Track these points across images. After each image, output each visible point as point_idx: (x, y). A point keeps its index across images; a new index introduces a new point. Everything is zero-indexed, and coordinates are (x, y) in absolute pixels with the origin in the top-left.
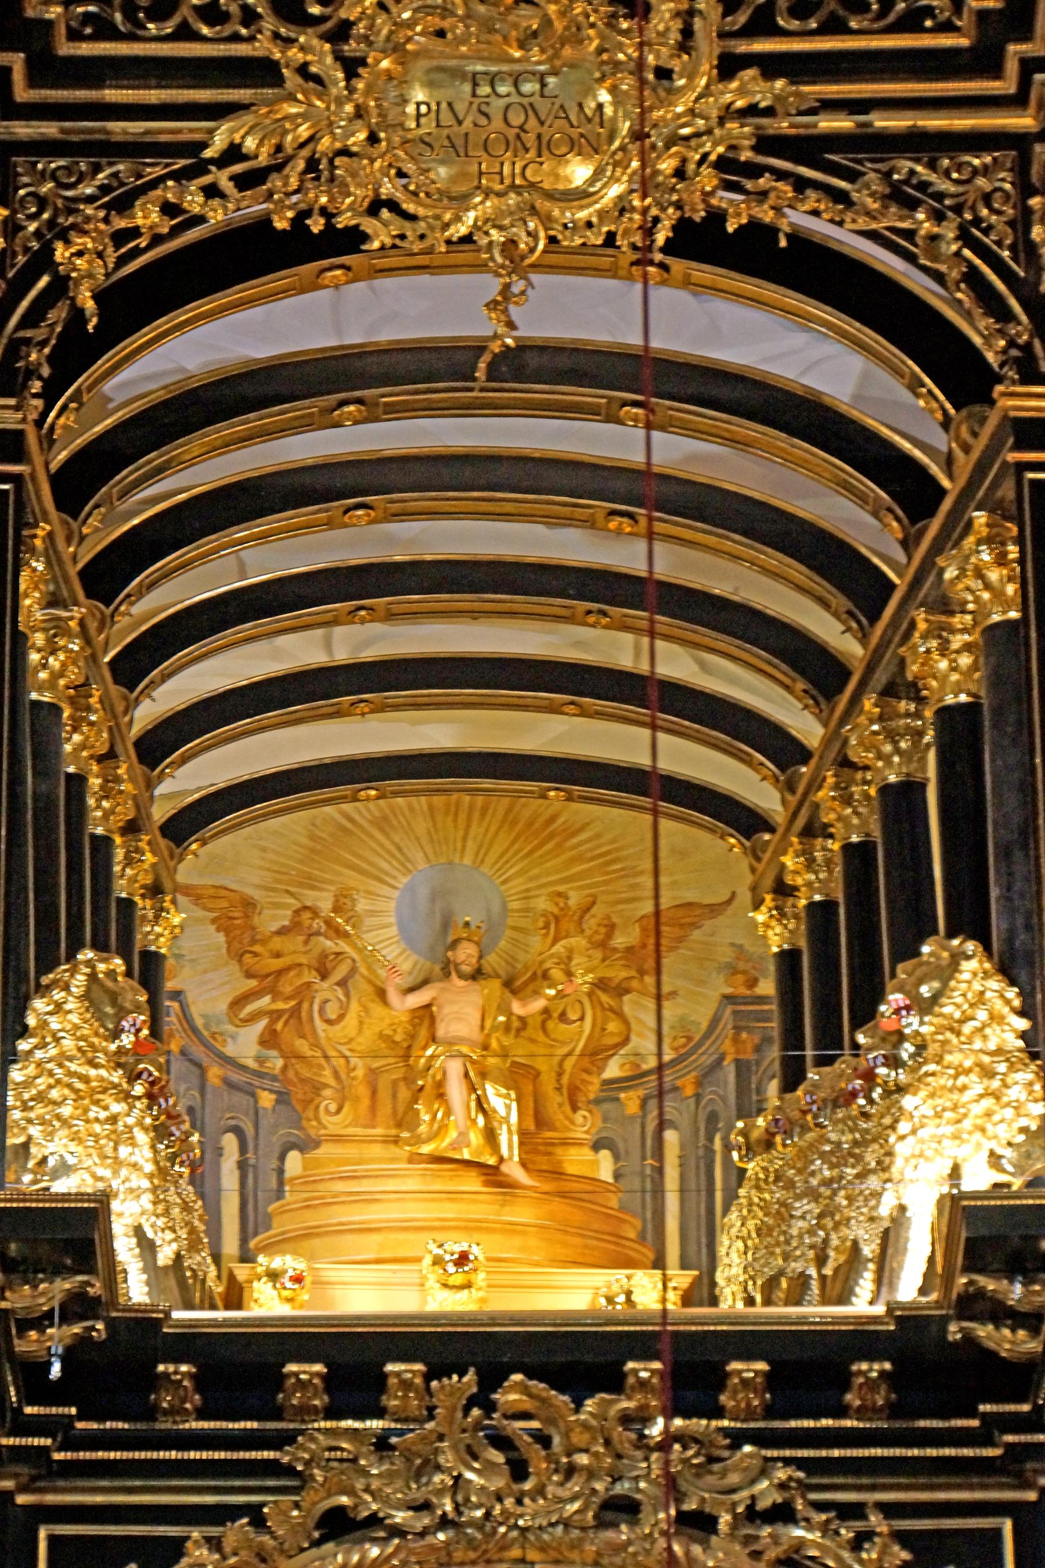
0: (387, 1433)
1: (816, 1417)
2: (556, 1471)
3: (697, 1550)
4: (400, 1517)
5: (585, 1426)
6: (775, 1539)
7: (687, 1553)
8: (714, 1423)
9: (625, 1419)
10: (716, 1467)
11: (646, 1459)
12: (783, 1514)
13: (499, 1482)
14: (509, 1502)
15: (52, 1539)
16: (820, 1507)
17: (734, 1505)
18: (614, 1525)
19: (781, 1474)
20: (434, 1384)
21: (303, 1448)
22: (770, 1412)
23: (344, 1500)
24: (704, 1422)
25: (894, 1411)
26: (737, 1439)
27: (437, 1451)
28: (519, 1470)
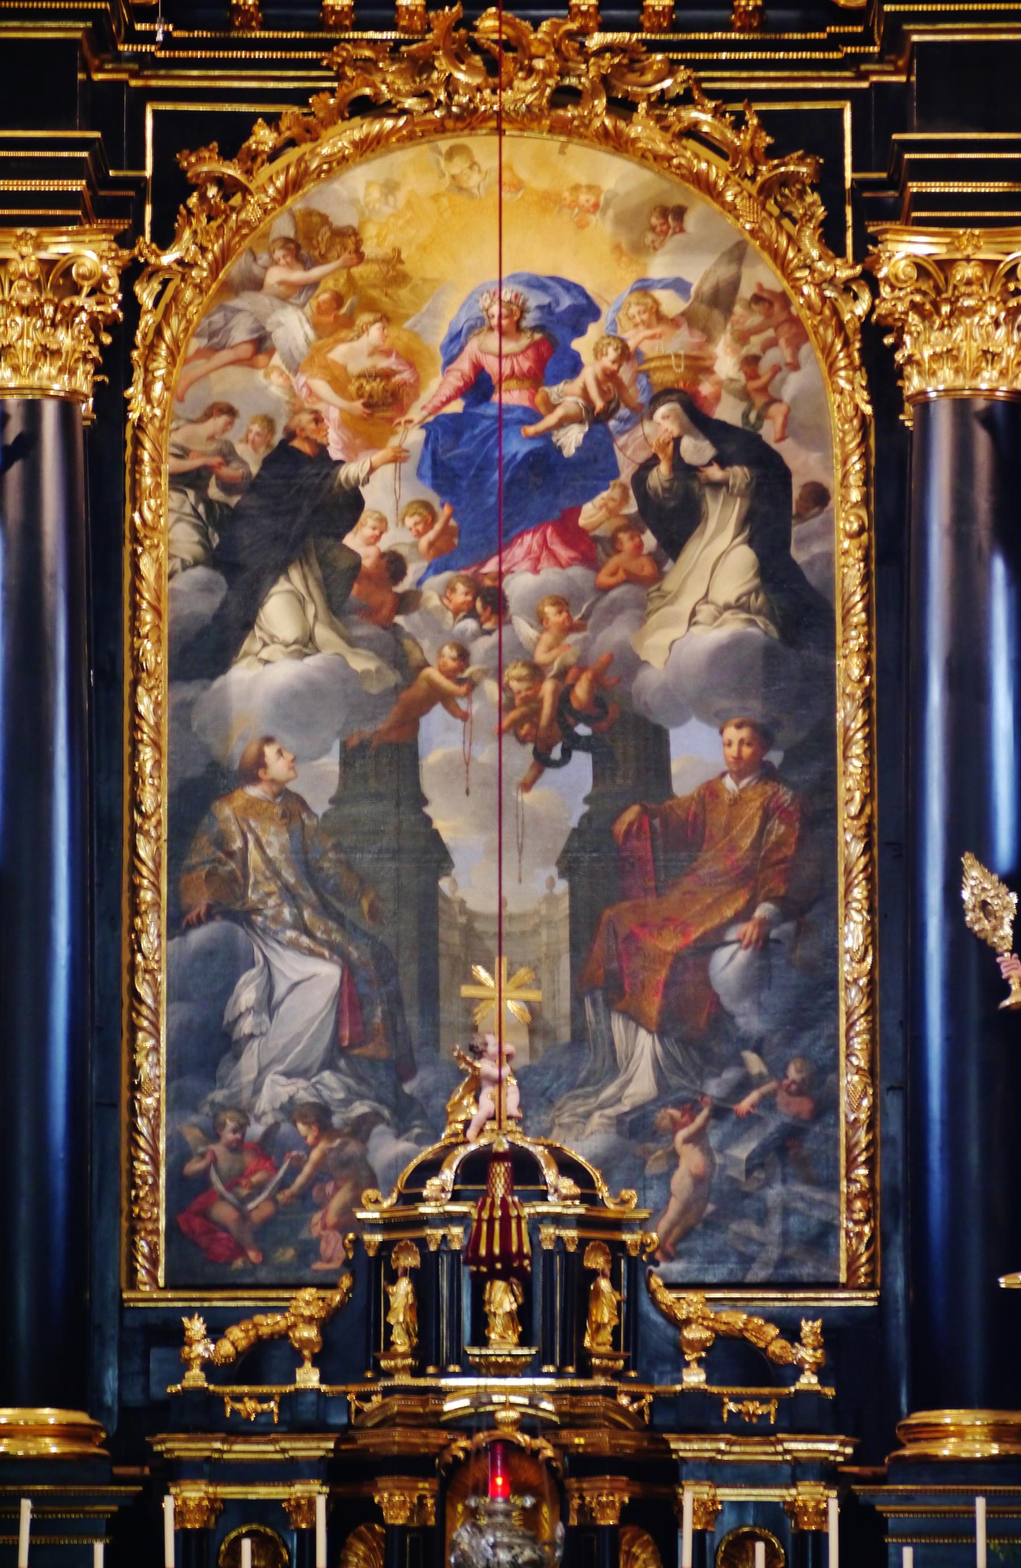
0: (398, 43)
1: (710, 31)
2: (521, 69)
3: (621, 124)
4: (409, 103)
5: (541, 41)
6: (680, 119)
7: (615, 127)
8: (635, 36)
9: (570, 35)
10: (637, 66)
11: (586, 62)
12: (685, 99)
13: (477, 81)
14: (487, 92)
15: (156, 113)
16: (711, 94)
17: (649, 96)
18: (564, 106)
19: (683, 74)
20: (432, 14)
21: (338, 55)
22: (675, 27)
23: (367, 91)
24: (627, 35)
25: (763, 27)
26: (654, 47)
27: (434, 58)
28: (493, 67)
